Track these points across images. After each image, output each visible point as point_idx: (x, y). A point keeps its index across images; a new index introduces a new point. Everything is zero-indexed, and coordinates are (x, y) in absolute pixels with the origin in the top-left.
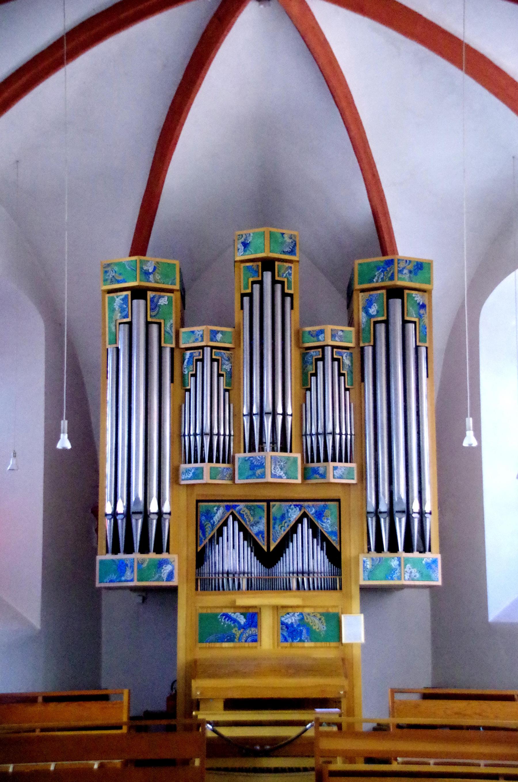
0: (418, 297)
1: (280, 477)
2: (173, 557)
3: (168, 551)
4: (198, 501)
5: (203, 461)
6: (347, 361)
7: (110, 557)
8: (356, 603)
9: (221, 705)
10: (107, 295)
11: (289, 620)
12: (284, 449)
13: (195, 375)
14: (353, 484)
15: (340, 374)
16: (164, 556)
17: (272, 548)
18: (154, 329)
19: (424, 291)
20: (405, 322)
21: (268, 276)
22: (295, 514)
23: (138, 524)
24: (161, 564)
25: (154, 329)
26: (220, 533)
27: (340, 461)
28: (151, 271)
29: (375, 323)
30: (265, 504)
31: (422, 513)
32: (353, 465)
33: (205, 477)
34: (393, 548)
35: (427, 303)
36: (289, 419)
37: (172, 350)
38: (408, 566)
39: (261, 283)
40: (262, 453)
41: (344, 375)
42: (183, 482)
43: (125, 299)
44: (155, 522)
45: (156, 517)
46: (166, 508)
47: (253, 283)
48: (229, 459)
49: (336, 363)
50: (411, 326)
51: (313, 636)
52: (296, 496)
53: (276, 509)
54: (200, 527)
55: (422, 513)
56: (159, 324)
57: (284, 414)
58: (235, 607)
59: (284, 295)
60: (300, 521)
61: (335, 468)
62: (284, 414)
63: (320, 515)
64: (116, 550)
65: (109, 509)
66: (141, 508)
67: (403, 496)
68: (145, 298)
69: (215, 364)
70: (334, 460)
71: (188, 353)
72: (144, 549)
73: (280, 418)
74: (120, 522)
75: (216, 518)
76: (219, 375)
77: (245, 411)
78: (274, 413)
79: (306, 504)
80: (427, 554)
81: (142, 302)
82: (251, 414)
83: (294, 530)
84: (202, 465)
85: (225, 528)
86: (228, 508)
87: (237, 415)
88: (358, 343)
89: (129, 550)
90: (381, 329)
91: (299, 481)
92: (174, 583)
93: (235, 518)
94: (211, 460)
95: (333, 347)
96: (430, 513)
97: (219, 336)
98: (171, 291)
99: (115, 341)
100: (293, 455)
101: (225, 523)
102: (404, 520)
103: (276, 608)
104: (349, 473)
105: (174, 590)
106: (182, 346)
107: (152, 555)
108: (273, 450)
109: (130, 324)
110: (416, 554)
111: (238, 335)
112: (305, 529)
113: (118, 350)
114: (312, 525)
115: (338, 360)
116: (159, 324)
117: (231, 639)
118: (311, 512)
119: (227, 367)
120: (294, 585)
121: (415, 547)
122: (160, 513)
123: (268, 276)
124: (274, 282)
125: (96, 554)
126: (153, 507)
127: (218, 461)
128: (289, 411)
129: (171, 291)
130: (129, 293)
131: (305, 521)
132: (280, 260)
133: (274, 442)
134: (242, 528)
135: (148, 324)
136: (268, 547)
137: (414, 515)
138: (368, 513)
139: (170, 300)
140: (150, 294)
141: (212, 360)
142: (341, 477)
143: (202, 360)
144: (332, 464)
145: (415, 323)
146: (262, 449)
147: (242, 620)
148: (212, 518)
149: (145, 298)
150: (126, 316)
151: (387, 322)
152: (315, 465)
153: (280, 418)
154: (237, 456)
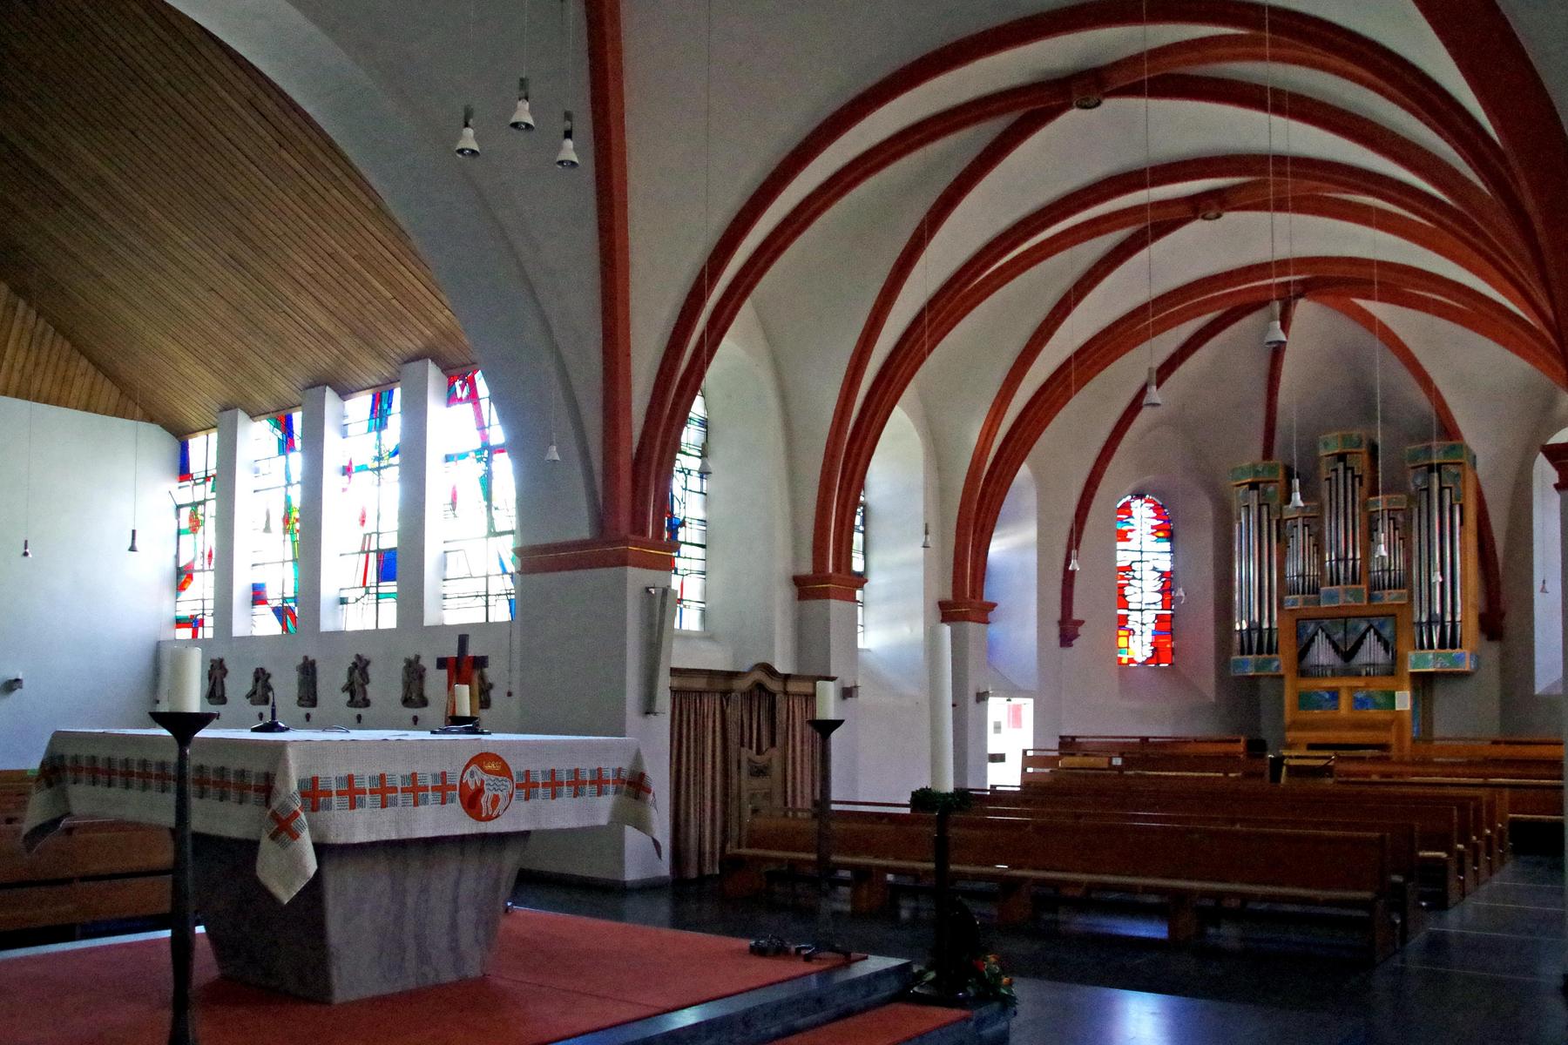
0: (1453, 469)
1: (1350, 602)
2: (1280, 656)
3: (1277, 653)
4: (1297, 620)
5: (1298, 593)
6: (1400, 518)
7: (1239, 657)
8: (1407, 684)
9: (1305, 747)
10: (1235, 488)
11: (1360, 695)
12: (1354, 582)
13: (1293, 537)
14: (1404, 605)
15: (1395, 529)
16: (1274, 655)
17: (1348, 649)
18: (1265, 509)
19: (1460, 464)
20: (1441, 489)
21: (1341, 466)
22: (1363, 626)
23: (1255, 636)
24: (1270, 662)
25: (1265, 509)
26: (1312, 640)
27: (1395, 588)
28: (1260, 470)
29: (1421, 490)
30: (1343, 620)
31: (1453, 622)
32: (1405, 591)
33: (1299, 604)
34: (1431, 646)
35: (1461, 472)
36: (1358, 562)
37: (1278, 522)
38: (1440, 658)
39: (1336, 470)
40: (1337, 587)
41: (1398, 529)
42: (1286, 608)
43: (1246, 492)
44: (1267, 635)
45: (1267, 631)
46: (1275, 626)
47: (1332, 470)
48: (1316, 591)
49: (1392, 522)
50: (1447, 491)
51: (1377, 706)
52: (1363, 613)
53: (1351, 622)
54: (1298, 636)
55: (1453, 622)
56: (1268, 505)
57: (1354, 559)
58: (1320, 688)
59: (1354, 477)
60: (1368, 630)
61: (1389, 594)
62: (1354, 559)
63: (1382, 625)
64: (1242, 653)
65: (1238, 627)
66: (1257, 625)
67: (1438, 611)
68: (1258, 488)
69: (1306, 528)
70: (1390, 588)
71: (1289, 522)
72: (1260, 652)
73: (1351, 563)
74: (1244, 635)
75: (1309, 631)
76: (1309, 535)
77: (1327, 559)
78: (1346, 559)
79: (1371, 619)
80: (1458, 650)
81: (1256, 492)
82: (1331, 561)
83: (1363, 636)
84: (1298, 596)
85: (1316, 637)
86: (1318, 624)
87: (1322, 562)
88: (1408, 505)
89: (1250, 653)
90: (1424, 494)
91: (1365, 602)
92: (1281, 672)
93: (1323, 631)
94: (1303, 593)
95: (1389, 510)
96: (1461, 621)
97: (1308, 510)
98: (1277, 482)
99: (1240, 518)
100: (1362, 586)
101: (1316, 634)
102: (1438, 627)
103: (1352, 689)
104: (1400, 597)
105: (1281, 677)
106: (1285, 517)
107: (1265, 656)
108: (1345, 584)
109: (1248, 506)
110: (1448, 651)
111: (1321, 508)
112: (1371, 638)
113: (1241, 523)
114: (1376, 633)
115: (1394, 519)
116: (1268, 505)
117: (1319, 707)
118: (1376, 624)
119: (1315, 529)
120: (1364, 673)
121: (1448, 645)
122: (1270, 629)
123: (1341, 466)
124: (1346, 469)
125: (1231, 654)
126: (1266, 625)
127: (1309, 593)
128: (1358, 556)
129: (1277, 482)
130: (1246, 486)
131: (1372, 631)
132: (1350, 453)
133: (1346, 578)
134: (1328, 637)
135: (1260, 506)
136: (1346, 648)
137: (1447, 624)
138: (1414, 623)
139: (1276, 487)
140: (1261, 486)
141: (1304, 526)
142: (1395, 599)
143: (1296, 526)
144: (1387, 591)
145: (1450, 488)
146: (1338, 583)
147: (1327, 696)
148: (1306, 630)
149: (1258, 488)
150: (1246, 502)
151: (1428, 490)
152: (1376, 592)
153: (1351, 563)
154: (1322, 589)
